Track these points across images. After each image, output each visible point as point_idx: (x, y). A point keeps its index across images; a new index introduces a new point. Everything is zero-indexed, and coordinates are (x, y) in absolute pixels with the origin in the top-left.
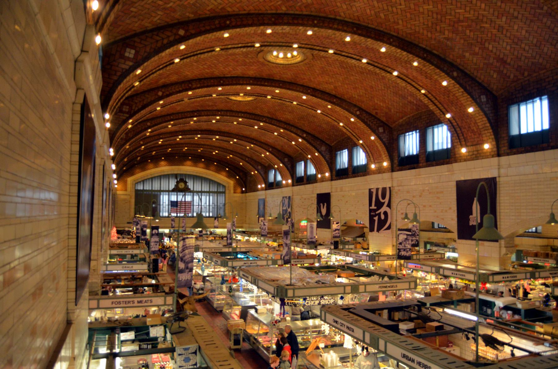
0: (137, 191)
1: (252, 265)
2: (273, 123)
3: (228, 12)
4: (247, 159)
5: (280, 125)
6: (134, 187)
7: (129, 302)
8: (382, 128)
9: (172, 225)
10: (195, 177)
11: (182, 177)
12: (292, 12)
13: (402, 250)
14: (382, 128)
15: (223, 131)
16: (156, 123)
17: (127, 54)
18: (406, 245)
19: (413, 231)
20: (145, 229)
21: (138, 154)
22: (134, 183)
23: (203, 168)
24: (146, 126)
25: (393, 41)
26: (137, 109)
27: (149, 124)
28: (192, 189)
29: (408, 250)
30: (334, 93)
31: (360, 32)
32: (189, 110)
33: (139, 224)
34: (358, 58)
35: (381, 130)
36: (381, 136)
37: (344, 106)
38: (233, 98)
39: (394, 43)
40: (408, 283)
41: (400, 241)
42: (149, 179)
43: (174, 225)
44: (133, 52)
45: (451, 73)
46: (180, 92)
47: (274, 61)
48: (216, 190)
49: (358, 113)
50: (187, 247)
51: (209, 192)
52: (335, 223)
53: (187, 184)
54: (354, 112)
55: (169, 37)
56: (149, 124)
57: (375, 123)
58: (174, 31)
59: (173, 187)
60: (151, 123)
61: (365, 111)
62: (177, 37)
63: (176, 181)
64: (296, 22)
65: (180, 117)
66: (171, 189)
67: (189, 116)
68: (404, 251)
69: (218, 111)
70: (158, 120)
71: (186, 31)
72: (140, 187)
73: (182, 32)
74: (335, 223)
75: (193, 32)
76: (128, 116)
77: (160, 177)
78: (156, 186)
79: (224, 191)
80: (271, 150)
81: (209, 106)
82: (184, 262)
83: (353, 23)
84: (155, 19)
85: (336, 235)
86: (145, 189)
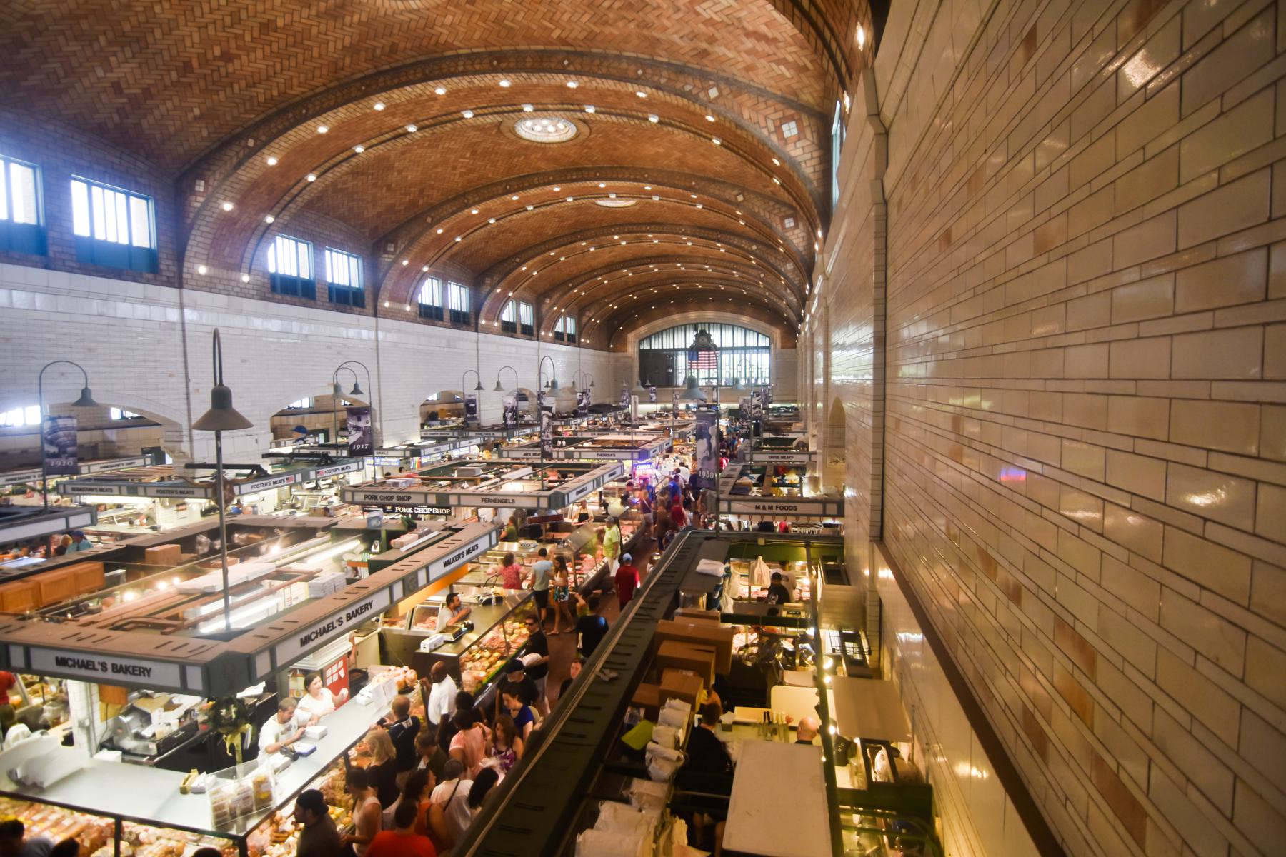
3: (297, 95)
8: (791, 220)
10: (722, 325)
12: (387, 67)
14: (791, 220)
17: (197, 188)
20: (472, 405)
25: (569, 65)
26: (403, 246)
27: (518, 260)
30: (687, 171)
31: (503, 65)
32: (567, 232)
34: (577, 107)
35: (789, 223)
36: (789, 234)
37: (712, 190)
38: (601, 202)
39: (571, 68)
42: (658, 333)
43: (654, 398)
44: (202, 183)
45: (702, 95)
46: (454, 213)
47: (545, 139)
49: (740, 198)
51: (757, 348)
54: (733, 199)
55: (237, 153)
56: (518, 260)
57: (776, 211)
58: (243, 143)
61: (754, 192)
62: (247, 150)
64: (396, 81)
69: (612, 226)
71: (256, 139)
72: (645, 346)
73: (251, 143)
75: (263, 138)
76: (393, 257)
77: (673, 329)
78: (666, 342)
80: (762, 275)
81: (593, 223)
83: (490, 54)
84: (205, 133)
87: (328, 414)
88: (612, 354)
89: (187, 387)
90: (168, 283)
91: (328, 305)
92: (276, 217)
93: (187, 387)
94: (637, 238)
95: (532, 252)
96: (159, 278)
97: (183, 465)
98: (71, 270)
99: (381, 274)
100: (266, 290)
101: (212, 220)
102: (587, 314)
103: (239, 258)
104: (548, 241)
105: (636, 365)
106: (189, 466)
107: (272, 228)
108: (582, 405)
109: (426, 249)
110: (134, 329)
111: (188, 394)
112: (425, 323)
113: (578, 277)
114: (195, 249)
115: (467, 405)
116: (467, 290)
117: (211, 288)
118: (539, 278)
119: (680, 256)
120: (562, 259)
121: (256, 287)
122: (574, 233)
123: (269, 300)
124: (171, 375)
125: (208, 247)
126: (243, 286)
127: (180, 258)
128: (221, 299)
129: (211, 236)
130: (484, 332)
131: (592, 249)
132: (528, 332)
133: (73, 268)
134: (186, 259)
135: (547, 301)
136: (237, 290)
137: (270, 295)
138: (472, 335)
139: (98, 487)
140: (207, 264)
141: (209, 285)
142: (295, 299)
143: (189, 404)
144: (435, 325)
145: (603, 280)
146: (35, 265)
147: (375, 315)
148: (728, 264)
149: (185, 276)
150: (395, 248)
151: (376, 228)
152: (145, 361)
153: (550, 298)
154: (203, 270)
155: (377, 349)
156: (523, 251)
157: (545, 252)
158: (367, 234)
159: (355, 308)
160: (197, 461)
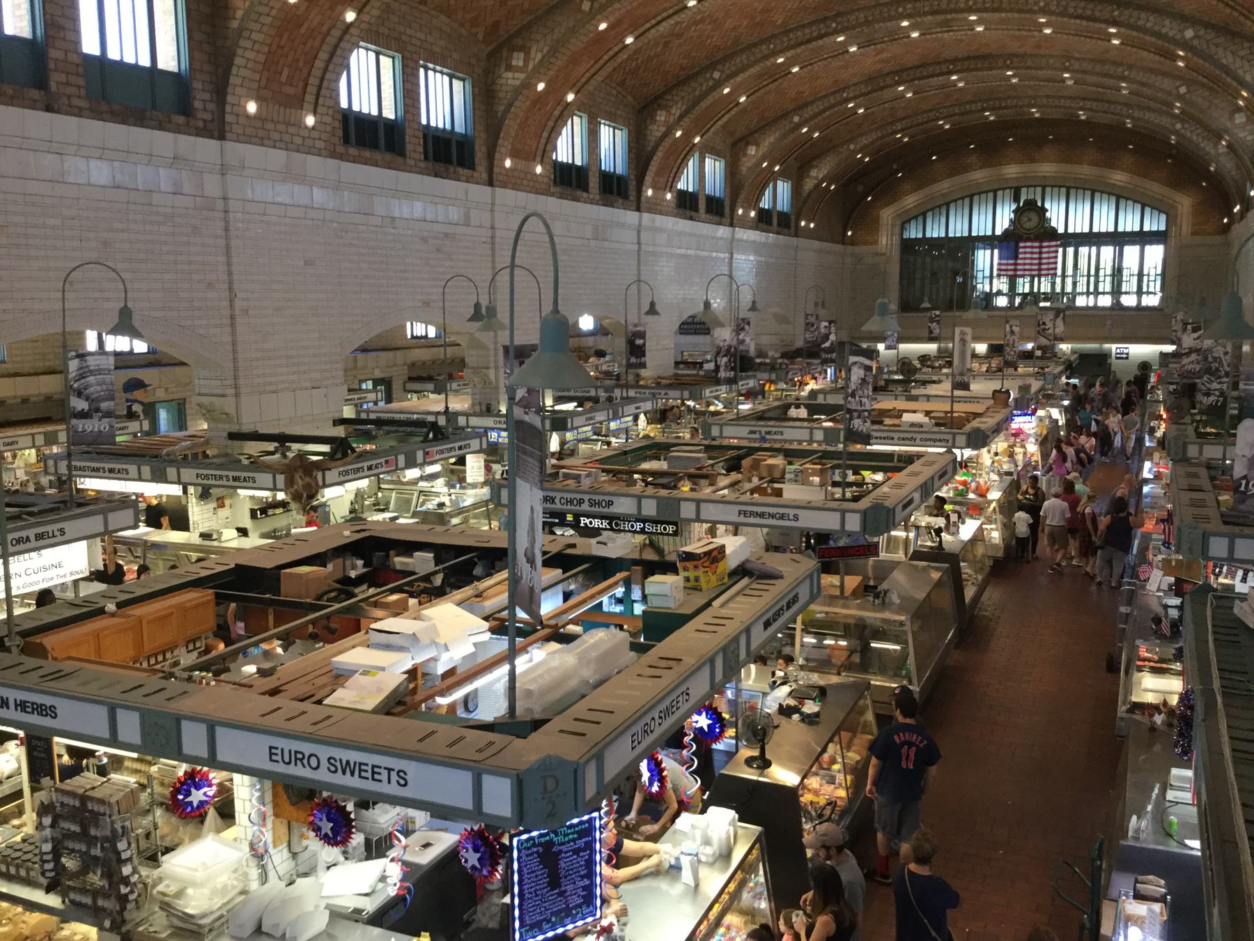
0: (908, 246)
1: (768, 437)
2: (1071, 10)
4: (1178, 126)
5: (1097, 14)
6: (897, 230)
7: (221, 478)
9: (931, 332)
11: (1031, 197)
13: (855, 414)
15: (1021, 51)
16: (734, 69)
18: (864, 400)
19: (1215, 359)
20: (639, 342)
21: (852, 147)
22: (899, 223)
23: (1096, 165)
24: (711, 83)
26: (539, 56)
28: (1061, 230)
29: (866, 414)
33: (743, 329)
40: (837, 515)
41: (854, 387)
48: (1137, 228)
50: (91, 371)
52: (1189, 327)
53: (1048, 214)
56: (716, 75)
59: (1006, 225)
60: (722, 72)
63: (1014, 207)
65: (792, 42)
66: (998, 232)
67: (815, 34)
68: (859, 417)
70: (738, 60)
72: (914, 233)
74: (1189, 327)
76: (523, 76)
78: (958, 228)
79: (1163, 228)
82: (87, 399)
85: (1190, 367)
86: (928, 235)
87: (391, 354)
88: (850, 248)
89: (232, 306)
90: (205, 131)
91: (423, 165)
92: (359, 12)
93: (232, 306)
94: (946, 25)
95: (742, 59)
96: (192, 122)
97: (225, 434)
98: (79, 112)
99: (502, 108)
100: (336, 140)
101: (268, 20)
102: (814, 173)
103: (301, 84)
104: (774, 36)
105: (894, 269)
106: (233, 436)
107: (352, 31)
108: (827, 344)
109: (574, 61)
110: (161, 210)
111: (232, 317)
112: (561, 197)
113: (812, 102)
114: (242, 72)
115: (631, 343)
116: (625, 132)
117: (263, 139)
118: (745, 110)
119: (1012, 56)
120: (795, 70)
121: (324, 136)
122: (825, 19)
123: (342, 157)
124: (210, 286)
125: (260, 67)
126: (306, 134)
127: (220, 91)
128: (277, 157)
129: (266, 49)
130: (650, 211)
131: (853, 49)
132: (717, 209)
133: (80, 109)
134: (230, 90)
135: (752, 150)
136: (298, 140)
137: (340, 149)
138: (631, 217)
139: (107, 466)
140: (258, 99)
141: (258, 133)
142: (377, 156)
143: (233, 334)
144: (577, 200)
145: (857, 107)
146: (33, 106)
147: (491, 183)
148: (1112, 70)
149: (228, 118)
150: (526, 61)
151: (496, 24)
152: (175, 262)
153: (757, 145)
154: (252, 107)
155: (493, 243)
156: (726, 59)
157: (766, 57)
158: (480, 36)
159: (460, 170)
160: (246, 428)
